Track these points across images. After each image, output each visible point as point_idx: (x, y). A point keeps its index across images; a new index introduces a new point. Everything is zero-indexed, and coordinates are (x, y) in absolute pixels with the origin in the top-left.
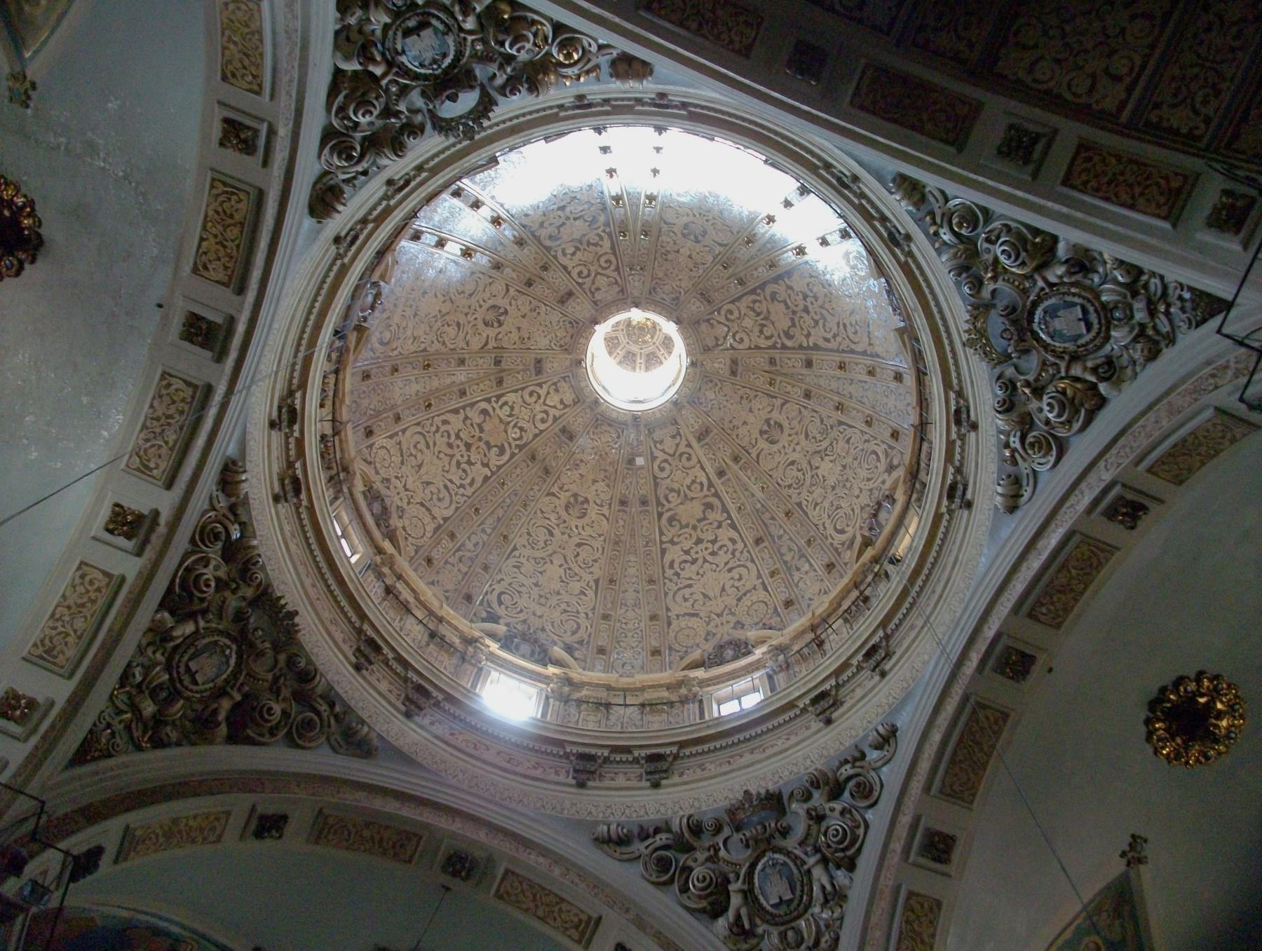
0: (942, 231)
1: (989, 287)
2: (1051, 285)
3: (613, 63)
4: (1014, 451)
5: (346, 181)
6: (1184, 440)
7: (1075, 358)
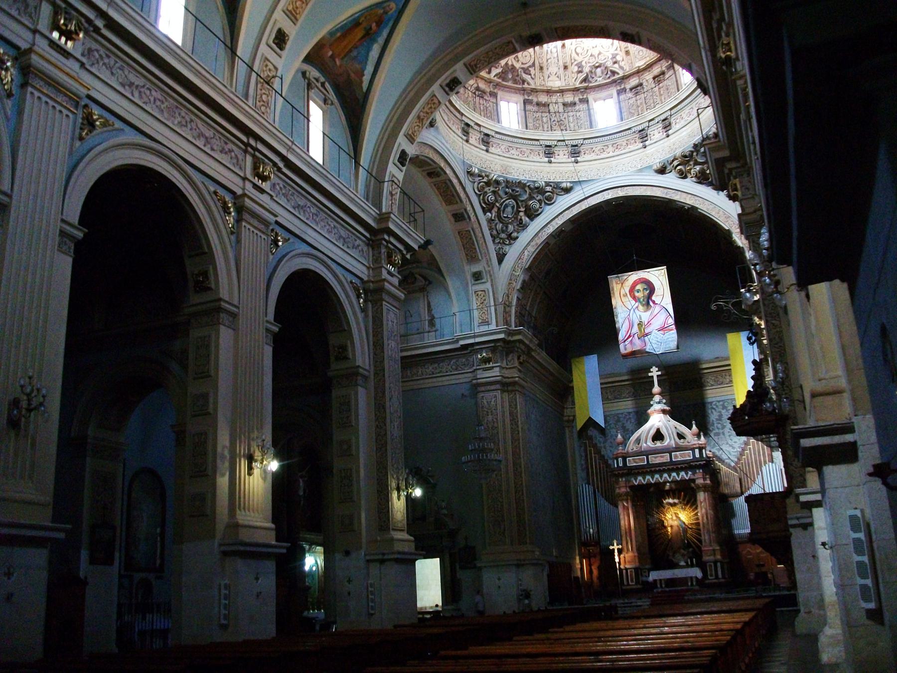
1: (528, 191)
3: (665, 168)
6: (474, 245)
7: (499, 209)
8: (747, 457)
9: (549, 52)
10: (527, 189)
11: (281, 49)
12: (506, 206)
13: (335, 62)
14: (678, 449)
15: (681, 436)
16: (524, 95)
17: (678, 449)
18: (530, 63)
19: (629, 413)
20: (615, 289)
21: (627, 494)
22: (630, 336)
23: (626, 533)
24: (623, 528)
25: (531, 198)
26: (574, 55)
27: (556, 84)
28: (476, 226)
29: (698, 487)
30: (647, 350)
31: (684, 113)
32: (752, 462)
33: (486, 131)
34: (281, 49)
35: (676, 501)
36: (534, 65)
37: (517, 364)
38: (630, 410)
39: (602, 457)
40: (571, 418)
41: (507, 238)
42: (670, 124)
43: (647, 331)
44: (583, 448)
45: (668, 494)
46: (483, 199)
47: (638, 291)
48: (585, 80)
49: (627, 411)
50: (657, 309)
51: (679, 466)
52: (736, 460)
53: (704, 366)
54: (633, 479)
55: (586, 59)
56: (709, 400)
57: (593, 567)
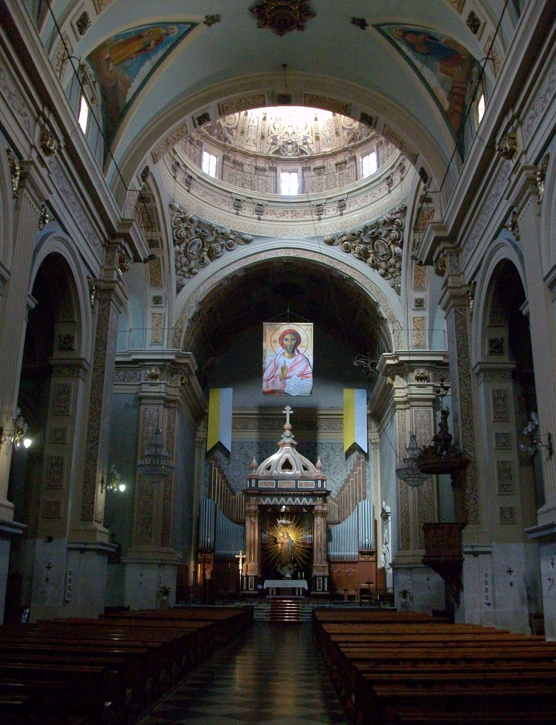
0: (234, 236)
2: (204, 251)
3: (334, 241)
4: (181, 214)
5: (398, 213)
7: (187, 245)
8: (346, 492)
9: (251, 120)
10: (214, 232)
11: (81, 33)
12: (194, 243)
13: (109, 66)
14: (303, 478)
15: (305, 469)
16: (224, 151)
17: (303, 478)
18: (234, 126)
19: (253, 443)
20: (267, 334)
21: (255, 512)
22: (273, 377)
23: (250, 545)
24: (248, 541)
25: (216, 241)
26: (272, 128)
27: (253, 149)
28: (166, 255)
29: (317, 513)
30: (286, 391)
31: (359, 199)
32: (349, 498)
33: (191, 174)
34: (81, 33)
35: (289, 522)
36: (236, 128)
37: (179, 384)
38: (254, 440)
39: (224, 477)
40: (202, 440)
41: (188, 272)
42: (345, 206)
43: (288, 375)
44: (208, 468)
45: (282, 515)
46: (176, 233)
47: (287, 340)
48: (277, 152)
49: (251, 440)
50: (300, 358)
51: (276, 493)
52: (337, 493)
53: (322, 412)
54: (262, 499)
55: (281, 135)
56: (321, 441)
57: (207, 572)
